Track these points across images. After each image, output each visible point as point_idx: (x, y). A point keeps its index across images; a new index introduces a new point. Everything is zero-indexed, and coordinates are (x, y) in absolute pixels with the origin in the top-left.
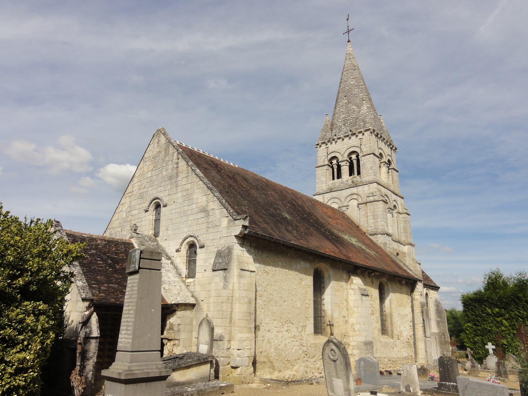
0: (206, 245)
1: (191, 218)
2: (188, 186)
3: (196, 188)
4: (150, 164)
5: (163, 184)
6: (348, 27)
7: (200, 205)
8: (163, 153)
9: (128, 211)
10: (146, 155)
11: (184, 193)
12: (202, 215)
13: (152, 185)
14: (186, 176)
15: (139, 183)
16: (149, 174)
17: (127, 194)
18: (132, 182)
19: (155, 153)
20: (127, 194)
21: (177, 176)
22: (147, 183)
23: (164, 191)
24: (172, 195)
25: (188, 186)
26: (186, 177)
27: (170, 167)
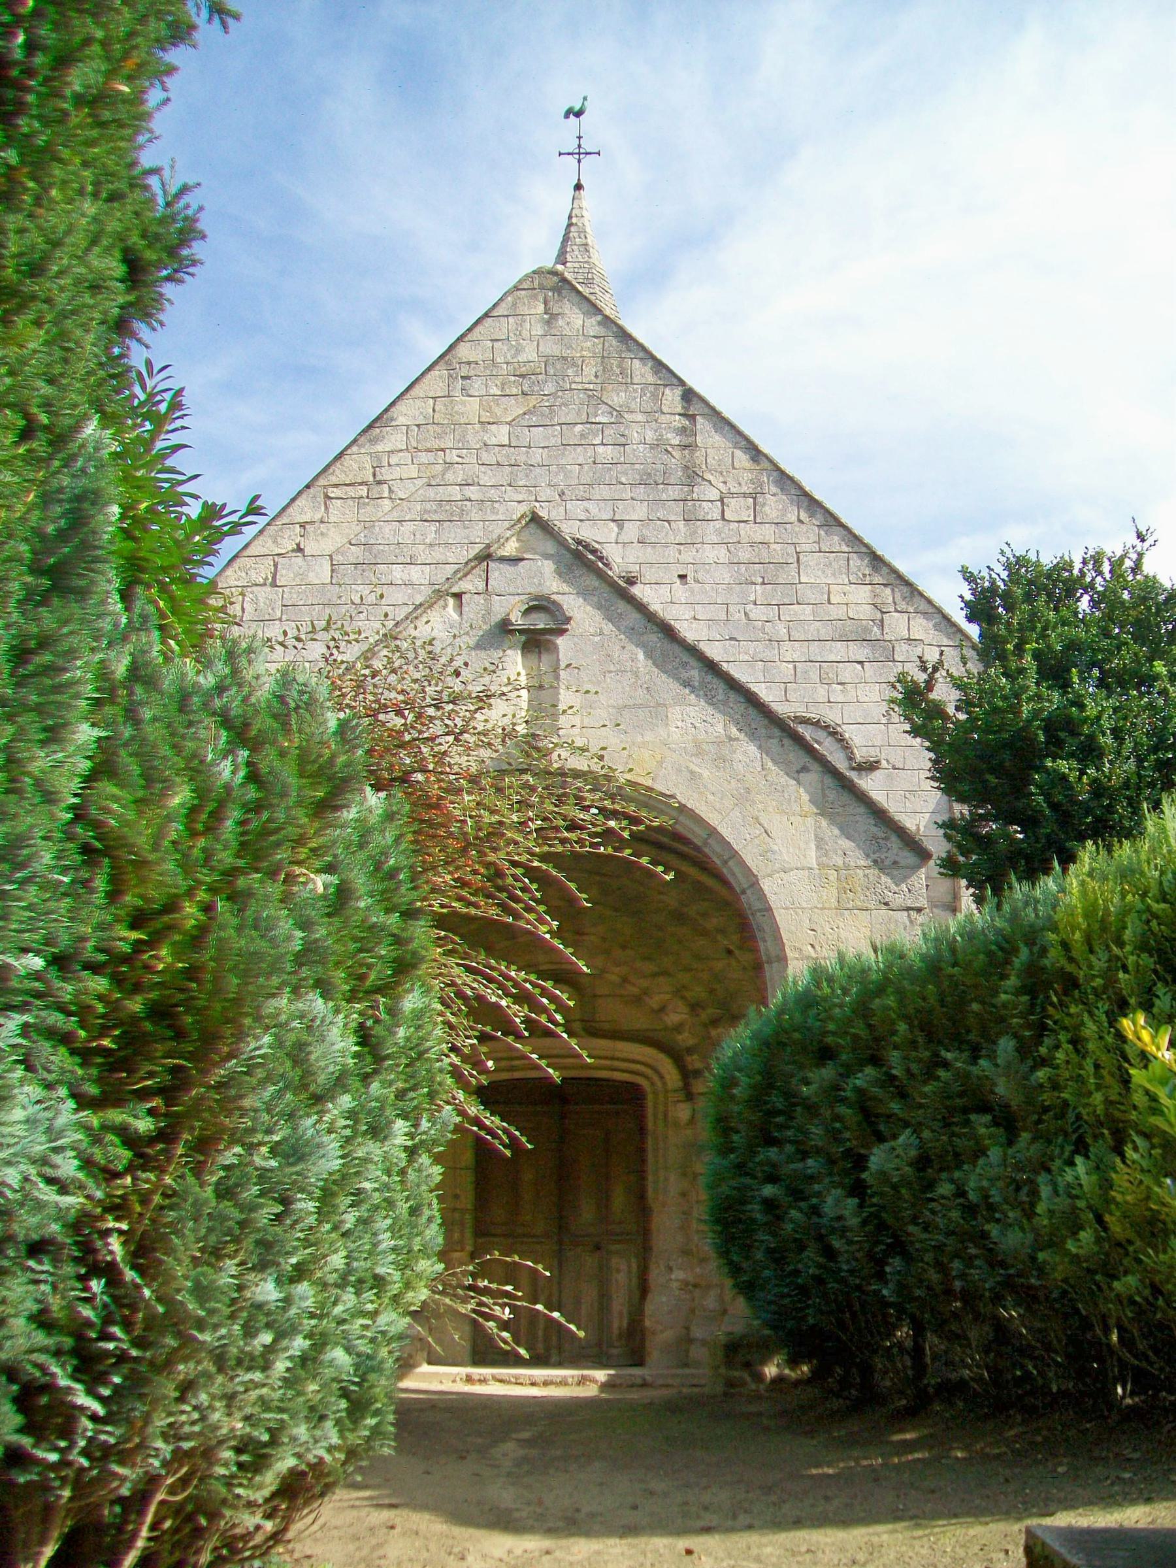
0: (884, 764)
1: (791, 652)
2: (767, 533)
3: (807, 548)
4: (495, 391)
5: (604, 491)
6: (579, 138)
7: (836, 612)
8: (590, 370)
9: (352, 560)
10: (464, 351)
11: (744, 554)
12: (859, 651)
13: (521, 483)
14: (744, 489)
15: (424, 458)
16: (501, 434)
17: (336, 486)
18: (374, 441)
19: (529, 354)
20: (336, 486)
21: (692, 476)
22: (483, 468)
23: (612, 524)
24: (666, 545)
25: (767, 533)
26: (745, 495)
27: (639, 433)
